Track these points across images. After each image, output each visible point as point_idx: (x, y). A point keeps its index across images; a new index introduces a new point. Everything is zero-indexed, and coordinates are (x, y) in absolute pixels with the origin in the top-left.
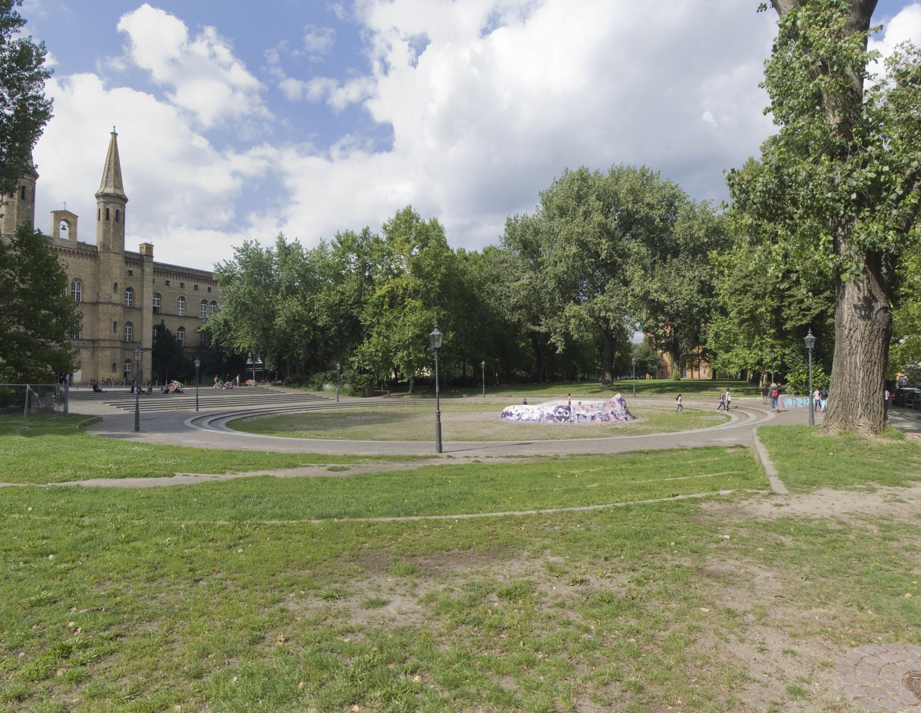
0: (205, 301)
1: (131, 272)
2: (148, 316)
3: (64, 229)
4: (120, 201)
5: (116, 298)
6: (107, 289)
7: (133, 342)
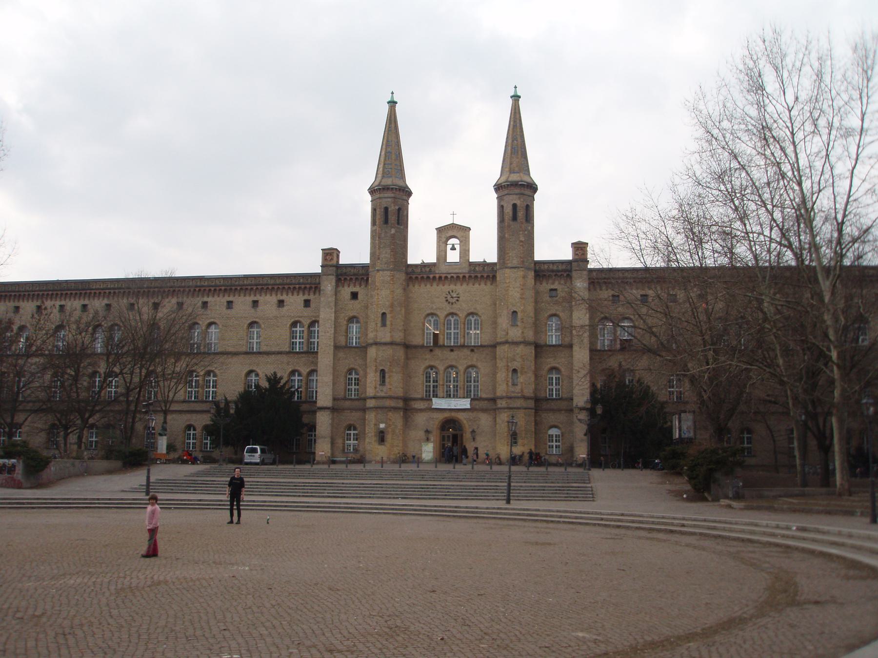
3: (453, 248)
4: (517, 191)
5: (515, 334)
6: (504, 321)
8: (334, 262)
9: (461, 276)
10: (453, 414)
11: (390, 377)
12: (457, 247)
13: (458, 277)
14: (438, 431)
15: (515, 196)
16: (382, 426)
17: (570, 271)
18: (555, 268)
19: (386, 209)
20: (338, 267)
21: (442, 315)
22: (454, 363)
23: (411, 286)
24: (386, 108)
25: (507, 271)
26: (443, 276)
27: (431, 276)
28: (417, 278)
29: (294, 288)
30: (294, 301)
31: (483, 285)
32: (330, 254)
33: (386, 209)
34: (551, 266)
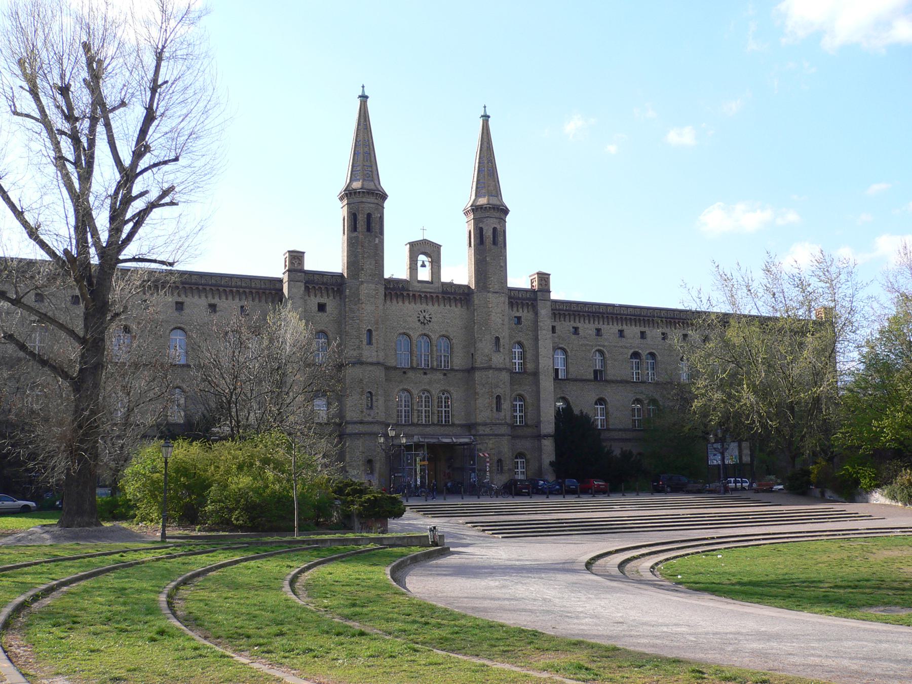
0: (636, 355)
1: (519, 318)
2: (547, 384)
3: (423, 266)
4: (497, 215)
12: (427, 264)
15: (495, 220)
17: (536, 300)
19: (369, 215)
22: (427, 387)
24: (358, 102)
25: (490, 295)
26: (417, 294)
31: (453, 307)
32: (296, 258)
33: (369, 215)
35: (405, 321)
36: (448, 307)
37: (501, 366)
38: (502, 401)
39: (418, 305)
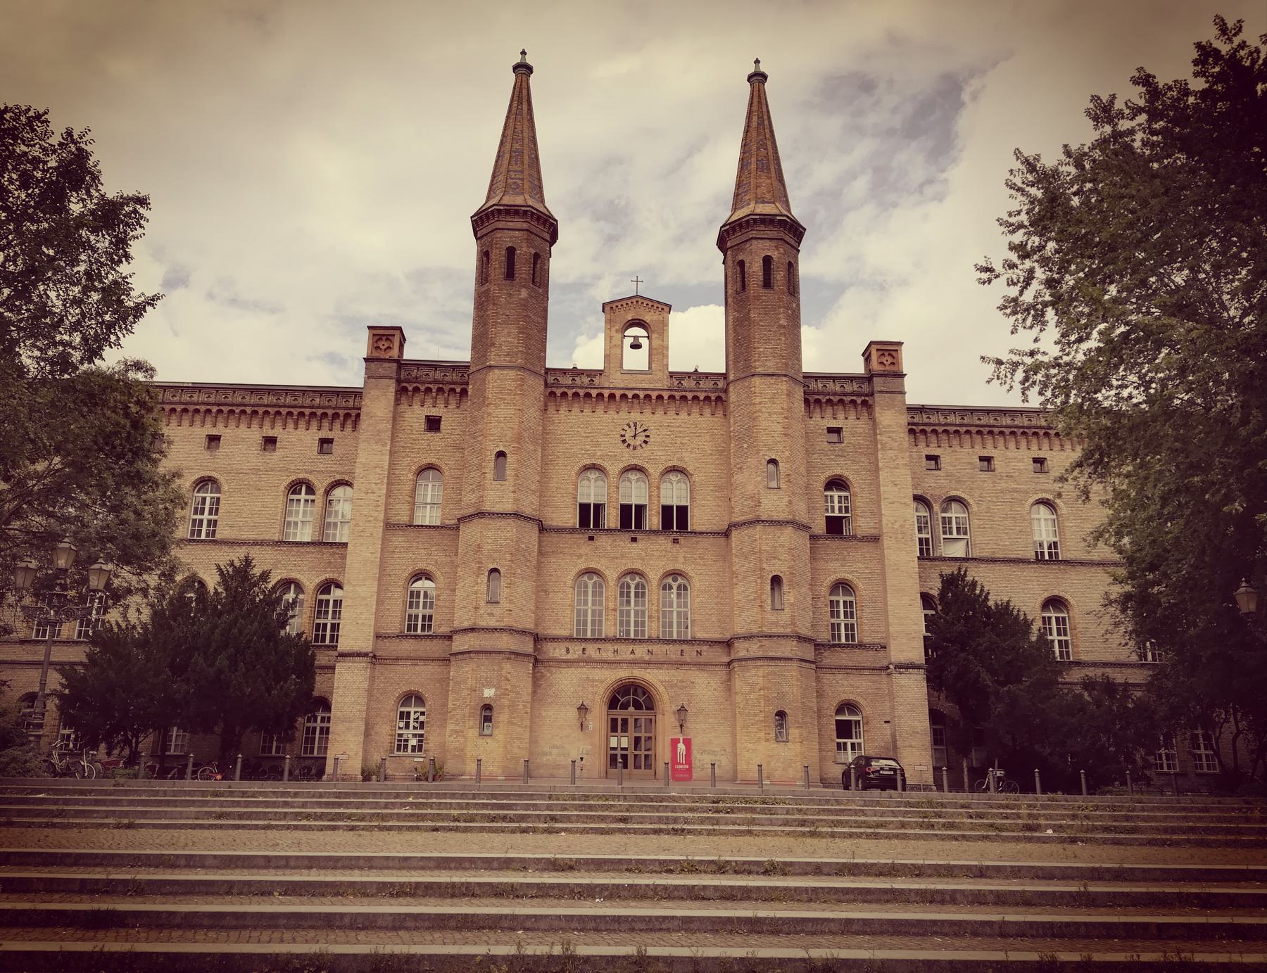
2: (901, 558)
3: (636, 346)
7: (861, 646)
8: (394, 353)
9: (654, 395)
10: (638, 673)
11: (509, 585)
12: (645, 342)
13: (648, 397)
14: (604, 708)
15: (768, 243)
16: (489, 693)
18: (838, 388)
19: (511, 251)
20: (401, 364)
21: (614, 469)
22: (637, 565)
23: (551, 410)
25: (757, 380)
26: (618, 393)
27: (594, 393)
28: (564, 395)
29: (302, 414)
30: (299, 442)
32: (385, 338)
33: (511, 251)
34: (831, 386)
35: (597, 445)
36: (683, 415)
37: (782, 517)
38: (785, 587)
39: (623, 414)
